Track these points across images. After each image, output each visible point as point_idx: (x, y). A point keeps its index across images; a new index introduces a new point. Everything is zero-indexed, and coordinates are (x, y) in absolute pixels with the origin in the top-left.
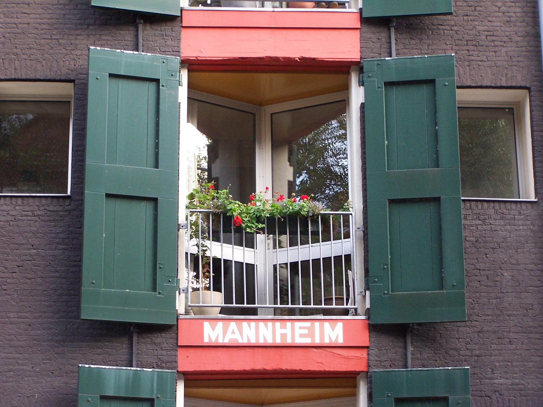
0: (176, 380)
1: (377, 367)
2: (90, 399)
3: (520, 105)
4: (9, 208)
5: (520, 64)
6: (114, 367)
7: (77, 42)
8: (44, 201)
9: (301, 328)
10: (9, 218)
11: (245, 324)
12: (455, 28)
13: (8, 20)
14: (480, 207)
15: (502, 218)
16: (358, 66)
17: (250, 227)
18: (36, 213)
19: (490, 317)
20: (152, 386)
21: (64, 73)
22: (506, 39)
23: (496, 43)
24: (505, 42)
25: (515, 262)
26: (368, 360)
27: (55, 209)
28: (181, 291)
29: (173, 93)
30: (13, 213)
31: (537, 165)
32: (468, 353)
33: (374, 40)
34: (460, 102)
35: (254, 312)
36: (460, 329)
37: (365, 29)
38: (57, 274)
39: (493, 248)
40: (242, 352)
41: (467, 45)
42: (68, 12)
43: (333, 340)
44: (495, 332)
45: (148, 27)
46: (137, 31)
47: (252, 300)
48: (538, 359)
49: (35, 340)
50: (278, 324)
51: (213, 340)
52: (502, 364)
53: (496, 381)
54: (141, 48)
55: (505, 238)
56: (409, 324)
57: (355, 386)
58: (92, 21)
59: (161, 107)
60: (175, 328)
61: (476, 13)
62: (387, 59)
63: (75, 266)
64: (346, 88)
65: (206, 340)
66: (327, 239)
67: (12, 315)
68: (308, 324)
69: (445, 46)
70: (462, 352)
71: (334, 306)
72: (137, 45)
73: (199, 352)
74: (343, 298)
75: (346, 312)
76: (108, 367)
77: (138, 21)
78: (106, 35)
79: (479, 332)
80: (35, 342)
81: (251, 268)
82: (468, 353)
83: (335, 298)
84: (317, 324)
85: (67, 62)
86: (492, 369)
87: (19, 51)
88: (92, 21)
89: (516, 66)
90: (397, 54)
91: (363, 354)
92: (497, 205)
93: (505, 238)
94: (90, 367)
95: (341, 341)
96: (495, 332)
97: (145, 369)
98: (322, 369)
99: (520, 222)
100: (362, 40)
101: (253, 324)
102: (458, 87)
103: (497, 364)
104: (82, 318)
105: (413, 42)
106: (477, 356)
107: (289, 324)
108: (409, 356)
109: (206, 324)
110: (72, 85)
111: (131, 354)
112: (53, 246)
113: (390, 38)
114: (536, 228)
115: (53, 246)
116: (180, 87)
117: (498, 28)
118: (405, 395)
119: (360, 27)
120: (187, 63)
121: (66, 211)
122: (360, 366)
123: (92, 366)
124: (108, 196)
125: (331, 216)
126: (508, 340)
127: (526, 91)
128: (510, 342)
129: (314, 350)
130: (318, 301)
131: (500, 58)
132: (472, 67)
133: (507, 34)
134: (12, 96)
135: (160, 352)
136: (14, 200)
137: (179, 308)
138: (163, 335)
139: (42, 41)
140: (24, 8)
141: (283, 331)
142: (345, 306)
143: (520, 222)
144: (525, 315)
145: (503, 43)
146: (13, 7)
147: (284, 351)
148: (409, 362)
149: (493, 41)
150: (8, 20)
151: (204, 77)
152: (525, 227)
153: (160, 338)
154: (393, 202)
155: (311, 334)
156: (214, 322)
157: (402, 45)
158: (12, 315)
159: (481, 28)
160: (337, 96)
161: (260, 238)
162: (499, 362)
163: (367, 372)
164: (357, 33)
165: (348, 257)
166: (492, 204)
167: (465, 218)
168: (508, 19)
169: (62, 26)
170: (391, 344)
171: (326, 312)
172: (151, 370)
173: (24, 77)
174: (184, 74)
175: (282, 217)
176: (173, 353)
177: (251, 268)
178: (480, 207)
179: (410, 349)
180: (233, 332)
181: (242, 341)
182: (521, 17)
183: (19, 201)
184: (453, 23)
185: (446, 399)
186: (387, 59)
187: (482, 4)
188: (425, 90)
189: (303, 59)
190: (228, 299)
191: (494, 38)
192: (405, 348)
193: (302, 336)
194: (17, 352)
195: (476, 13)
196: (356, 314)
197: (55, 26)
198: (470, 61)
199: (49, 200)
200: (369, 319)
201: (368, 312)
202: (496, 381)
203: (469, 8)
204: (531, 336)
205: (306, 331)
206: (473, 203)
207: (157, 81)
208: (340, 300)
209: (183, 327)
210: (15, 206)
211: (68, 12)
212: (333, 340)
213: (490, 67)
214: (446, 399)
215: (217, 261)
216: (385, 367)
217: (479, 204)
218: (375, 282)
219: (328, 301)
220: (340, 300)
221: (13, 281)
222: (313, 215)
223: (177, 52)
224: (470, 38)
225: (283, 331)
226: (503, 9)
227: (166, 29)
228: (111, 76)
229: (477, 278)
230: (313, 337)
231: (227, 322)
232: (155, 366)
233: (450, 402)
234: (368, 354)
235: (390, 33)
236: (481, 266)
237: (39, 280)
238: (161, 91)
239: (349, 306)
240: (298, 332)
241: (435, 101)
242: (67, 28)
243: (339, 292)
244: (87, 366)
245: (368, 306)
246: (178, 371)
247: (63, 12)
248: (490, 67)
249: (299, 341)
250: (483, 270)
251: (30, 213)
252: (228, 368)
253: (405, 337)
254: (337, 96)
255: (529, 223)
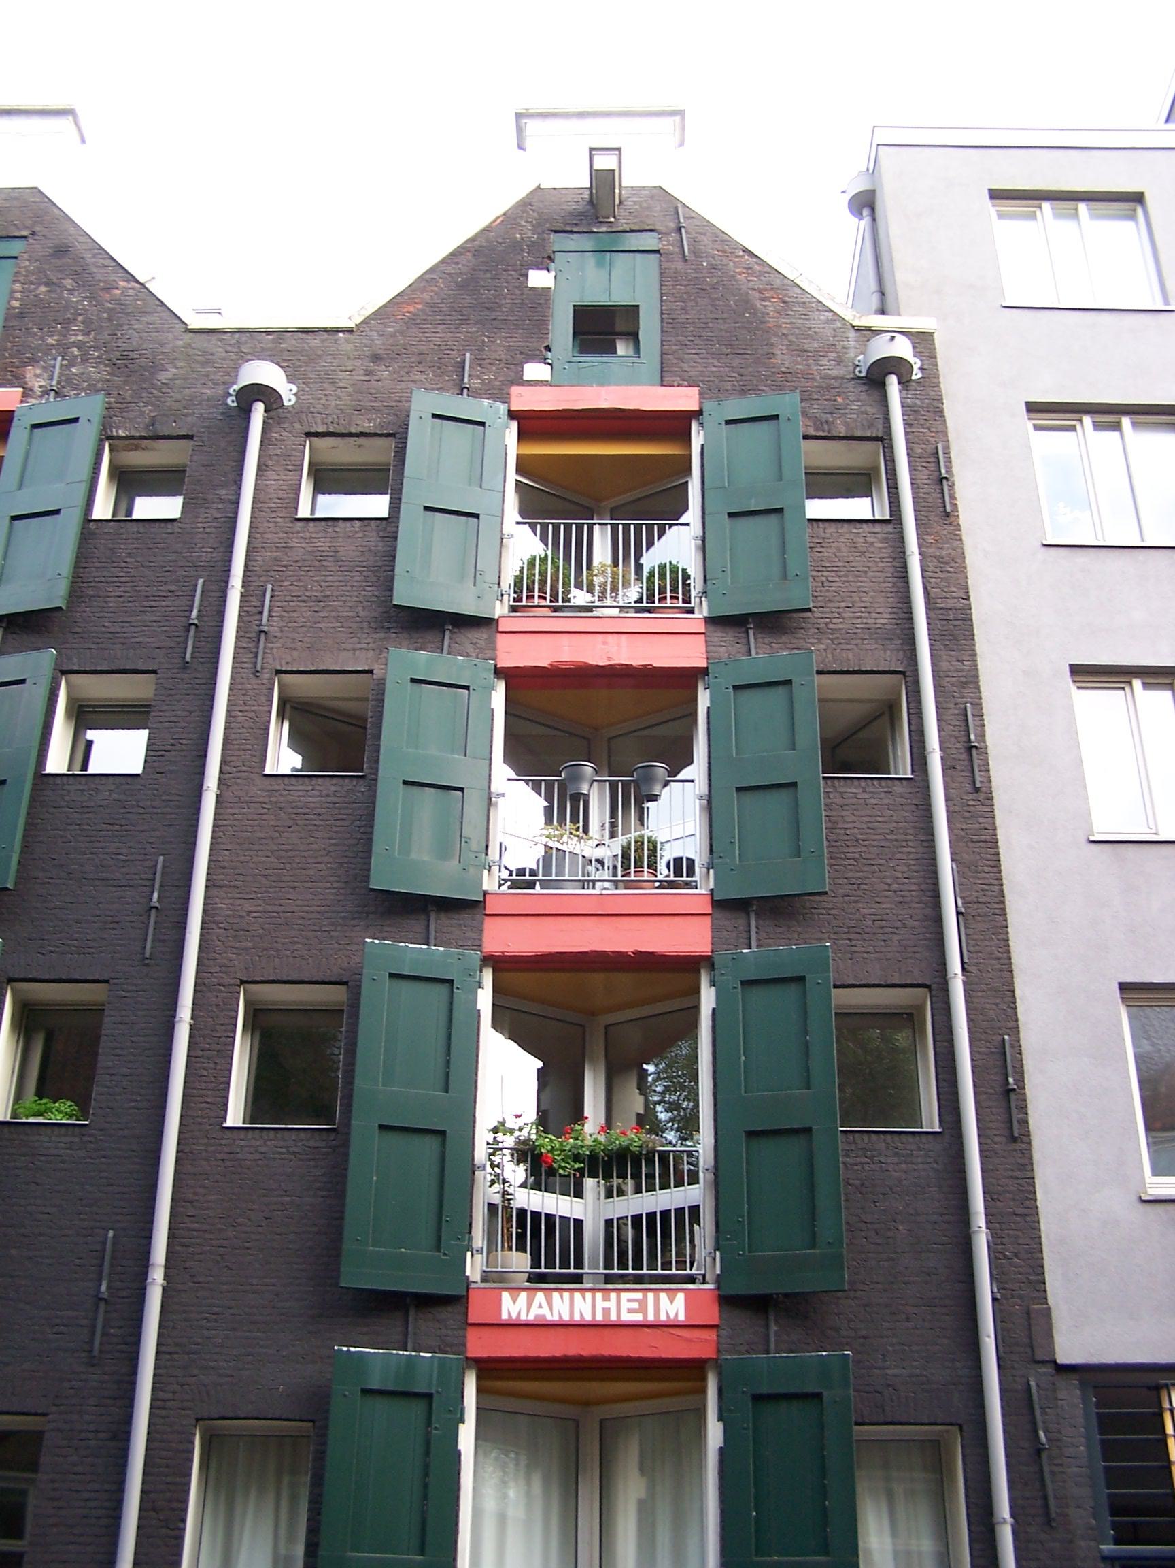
0: (464, 1369)
1: (730, 1353)
2: (347, 1393)
3: (921, 1008)
4: (258, 1143)
5: (917, 955)
6: (381, 1351)
7: (353, 934)
8: (302, 1135)
9: (629, 1300)
10: (258, 1156)
11: (556, 1295)
12: (832, 912)
13: (269, 908)
14: (866, 1141)
15: (896, 1155)
16: (706, 961)
17: (563, 1168)
18: (291, 1150)
19: (880, 1286)
20: (431, 1376)
21: (334, 973)
22: (898, 924)
23: (886, 930)
24: (897, 928)
25: (912, 1212)
26: (718, 1343)
27: (316, 1145)
28: (475, 1252)
29: (471, 997)
30: (263, 1149)
31: (941, 1085)
32: (852, 1334)
33: (729, 929)
34: (838, 1007)
35: (578, 1279)
36: (841, 1301)
37: (717, 915)
38: (315, 1229)
39: (884, 1194)
40: (552, 1331)
41: (848, 933)
42: (342, 897)
43: (672, 1316)
44: (887, 1306)
45: (442, 915)
46: (429, 921)
47: (579, 1264)
48: (946, 1341)
49: (283, 1314)
50: (599, 1295)
51: (514, 1316)
52: (897, 1348)
53: (889, 1372)
54: (432, 941)
55: (900, 1181)
56: (771, 1295)
57: (704, 1379)
58: (372, 909)
59: (455, 1014)
60: (465, 1300)
61: (860, 893)
62: (744, 951)
63: (337, 1219)
64: (697, 991)
65: (505, 1316)
66: (665, 1186)
67: (255, 1282)
68: (639, 1295)
69: (820, 935)
70: (844, 1333)
71: (674, 1271)
72: (428, 938)
73: (495, 1331)
74: (686, 1262)
75: (691, 1279)
76: (372, 1351)
77: (430, 908)
78: (389, 925)
79: (866, 1305)
80: (283, 1317)
81: (579, 1223)
82: (852, 1334)
83: (676, 1262)
84: (650, 1296)
85: (339, 960)
86: (883, 1355)
87: (279, 946)
88: (372, 909)
89: (910, 958)
90: (758, 946)
91: (712, 1335)
92: (888, 1137)
93: (900, 1181)
94: (348, 1350)
95: (682, 1317)
96: (887, 1306)
97: (422, 1354)
98: (656, 1355)
99: (919, 1160)
100: (715, 929)
101: (566, 1295)
102: (835, 986)
103: (890, 1348)
104: (343, 1285)
105: (779, 930)
106: (864, 1337)
107: (613, 1295)
108: (772, 1339)
109: (505, 1295)
110: (344, 988)
111: (406, 1334)
112: (312, 1193)
113: (749, 925)
114: (940, 1167)
115: (312, 1193)
116: (480, 990)
117: (888, 911)
118: (764, 1390)
119: (710, 912)
120: (489, 960)
121: (330, 1147)
122: (707, 1352)
123: (352, 1349)
124: (383, 1128)
125: (671, 1154)
126: (904, 1316)
127: (926, 990)
128: (908, 1318)
129: (647, 1330)
130: (666, 1265)
131: (889, 949)
132: (854, 961)
133: (900, 918)
134: (274, 1003)
135: (444, 1331)
136: (265, 1132)
137: (472, 1273)
138: (449, 1309)
139: (310, 934)
140: (289, 893)
141: (606, 1304)
142: (688, 1271)
143: (919, 1160)
144: (927, 1283)
145: (895, 930)
146: (275, 892)
147: (607, 1331)
148: (772, 1346)
149: (882, 927)
150: (269, 908)
151: (514, 978)
152: (926, 1166)
153: (445, 1313)
154: (751, 1134)
155: (643, 1309)
156: (515, 1293)
157: (765, 934)
158: (255, 1282)
159: (865, 911)
160: (686, 1002)
161: (589, 1183)
162: (893, 1345)
163: (717, 1360)
164: (708, 920)
165: (695, 1210)
166: (882, 1136)
167: (847, 1155)
168: (901, 899)
169: (334, 915)
170: (748, 1321)
171: (639, 1279)
172: (429, 1355)
173: (285, 978)
174: (488, 977)
175: (606, 1155)
176: (461, 1332)
177: (579, 1223)
178: (866, 1141)
179: (774, 1328)
180: (540, 1306)
181: (552, 1317)
182: (917, 896)
183: (272, 1134)
184: (830, 906)
185: (819, 1396)
186: (744, 951)
187: (867, 881)
188: (793, 989)
189: (637, 953)
190: (536, 1263)
191: (884, 923)
192: (767, 1326)
193: (630, 1311)
194: (259, 1331)
195: (860, 893)
196: (704, 1282)
197: (327, 915)
198: (852, 953)
199: (309, 1134)
200: (718, 1288)
201: (719, 1280)
202: (889, 1372)
203: (850, 887)
204: (936, 1310)
205: (635, 1305)
206: (857, 1135)
207: (451, 982)
208: (681, 1264)
209: (474, 1298)
210: (266, 1141)
211: (342, 897)
212: (672, 1316)
213: (878, 959)
214: (819, 1396)
215: (522, 1213)
216: (740, 1353)
217: (865, 1137)
218: (728, 1239)
219: (666, 1265)
220: (681, 1264)
221: (258, 1237)
222: (648, 1152)
223: (479, 946)
224: (853, 923)
225: (606, 1304)
226: (895, 886)
227: (465, 917)
228: (392, 975)
229: (863, 1234)
230: (645, 1312)
231: (532, 1292)
232: (437, 1350)
233: (825, 1398)
234: (718, 1336)
235: (749, 920)
236: (868, 1218)
237: (292, 1236)
238: (455, 995)
239: (694, 1271)
240: (625, 1305)
241: (805, 1004)
242: (341, 918)
243: (680, 1253)
244: (345, 1349)
245: (718, 1272)
246: (467, 1358)
247: (337, 897)
248: (878, 959)
249: (626, 1317)
250: (871, 1223)
251: (284, 1150)
252: (532, 1353)
253: (766, 1312)
254: (686, 1002)
255: (931, 1160)
